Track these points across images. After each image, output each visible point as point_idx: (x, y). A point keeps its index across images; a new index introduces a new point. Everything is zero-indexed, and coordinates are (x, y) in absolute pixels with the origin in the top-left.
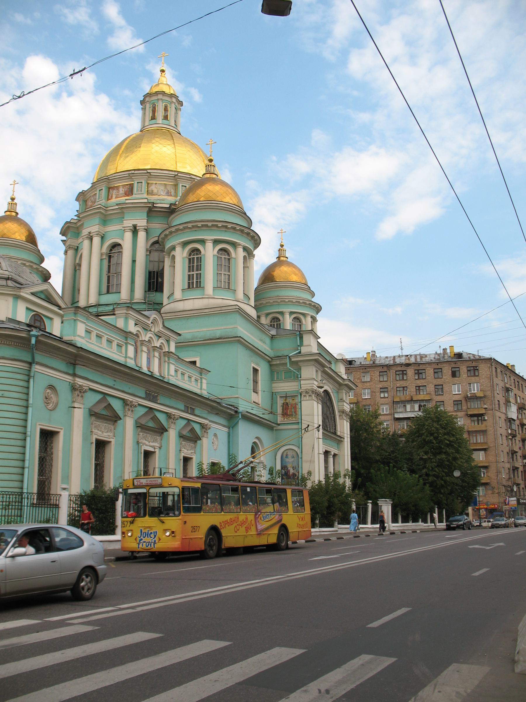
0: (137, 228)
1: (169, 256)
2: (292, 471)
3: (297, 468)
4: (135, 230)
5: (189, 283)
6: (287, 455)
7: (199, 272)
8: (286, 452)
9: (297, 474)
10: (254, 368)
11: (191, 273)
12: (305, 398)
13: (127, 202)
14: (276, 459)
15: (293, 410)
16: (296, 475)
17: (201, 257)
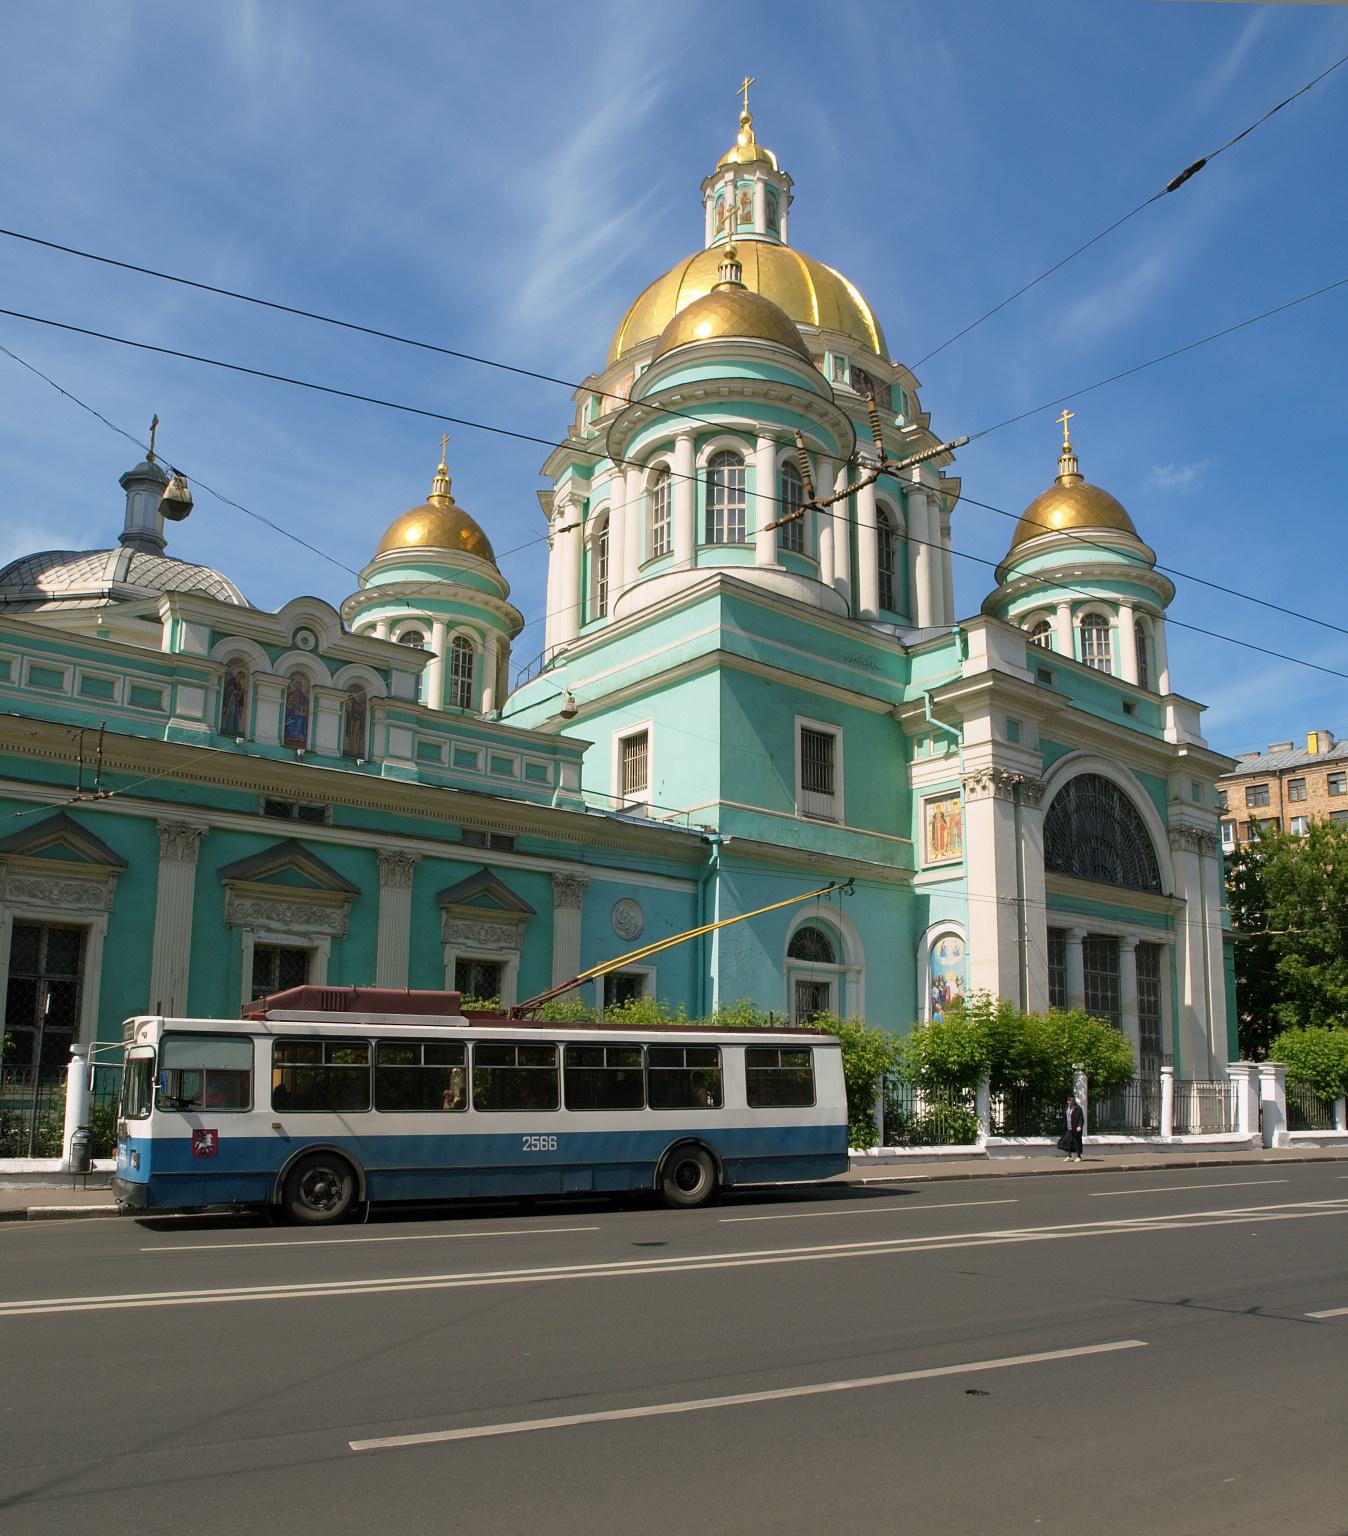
2: (954, 991)
6: (943, 953)
8: (939, 945)
10: (807, 733)
11: (660, 524)
12: (973, 796)
14: (916, 960)
15: (955, 831)
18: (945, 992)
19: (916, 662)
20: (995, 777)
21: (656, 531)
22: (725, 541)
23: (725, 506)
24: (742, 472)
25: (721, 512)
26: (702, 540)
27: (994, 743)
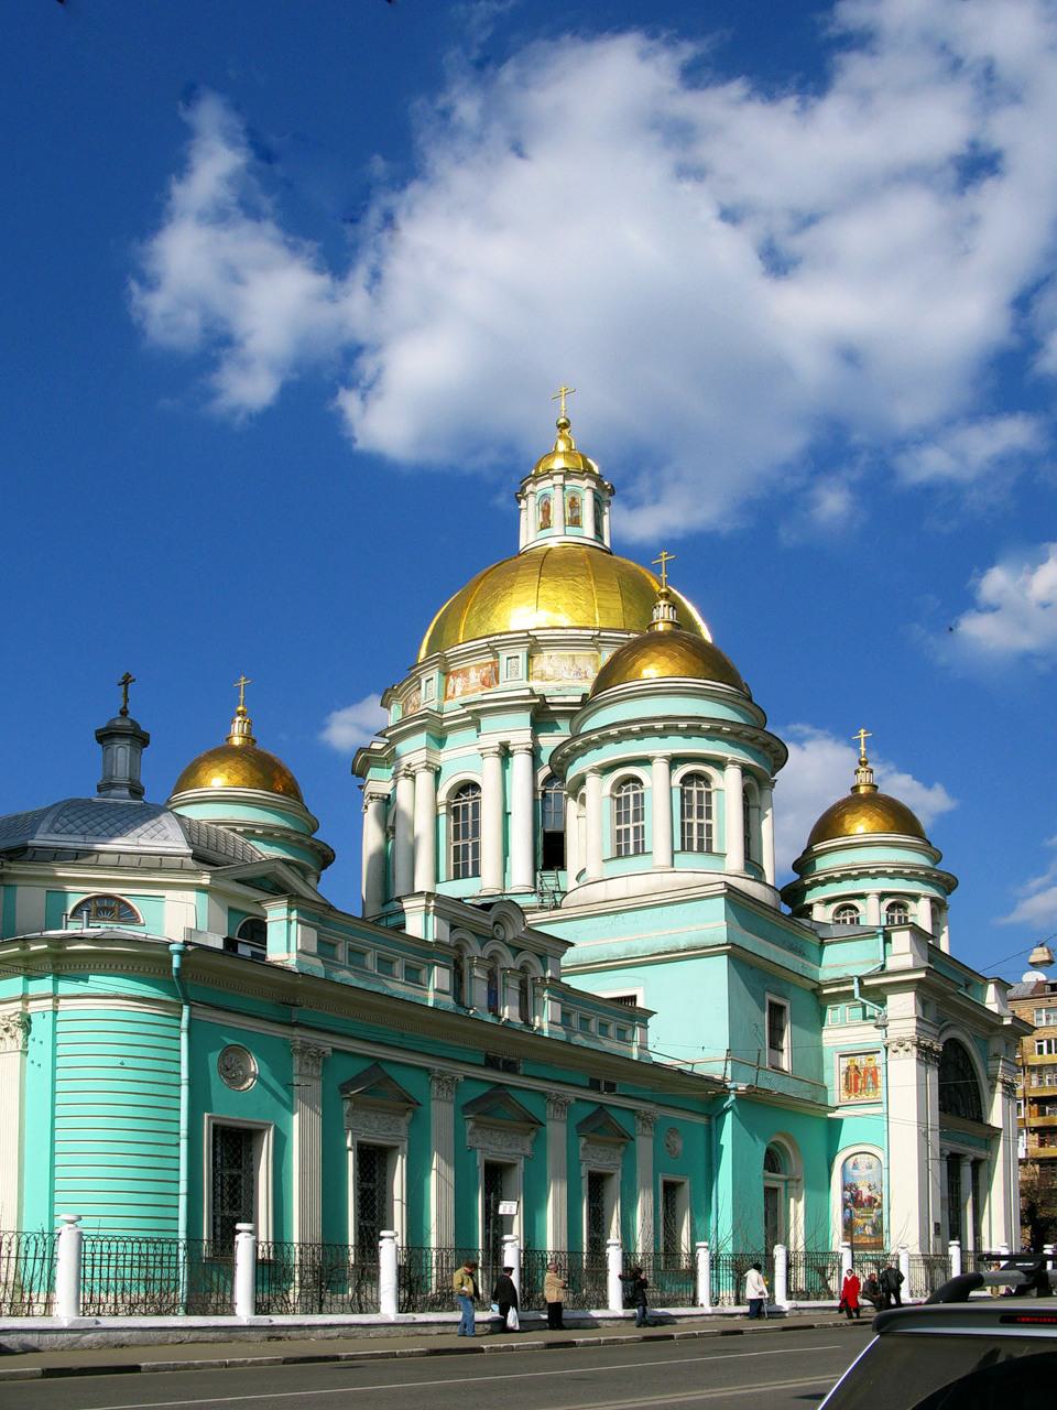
0: (511, 748)
1: (576, 796)
2: (866, 1193)
3: (878, 1185)
4: (505, 753)
5: (619, 847)
6: (855, 1166)
7: (641, 823)
9: (879, 1198)
11: (623, 827)
13: (486, 697)
16: (876, 1201)
17: (643, 794)
18: (858, 1194)
19: (828, 949)
20: (918, 1045)
21: (619, 832)
22: (695, 849)
23: (695, 821)
24: (709, 794)
25: (690, 825)
26: (678, 847)
27: (918, 1019)
